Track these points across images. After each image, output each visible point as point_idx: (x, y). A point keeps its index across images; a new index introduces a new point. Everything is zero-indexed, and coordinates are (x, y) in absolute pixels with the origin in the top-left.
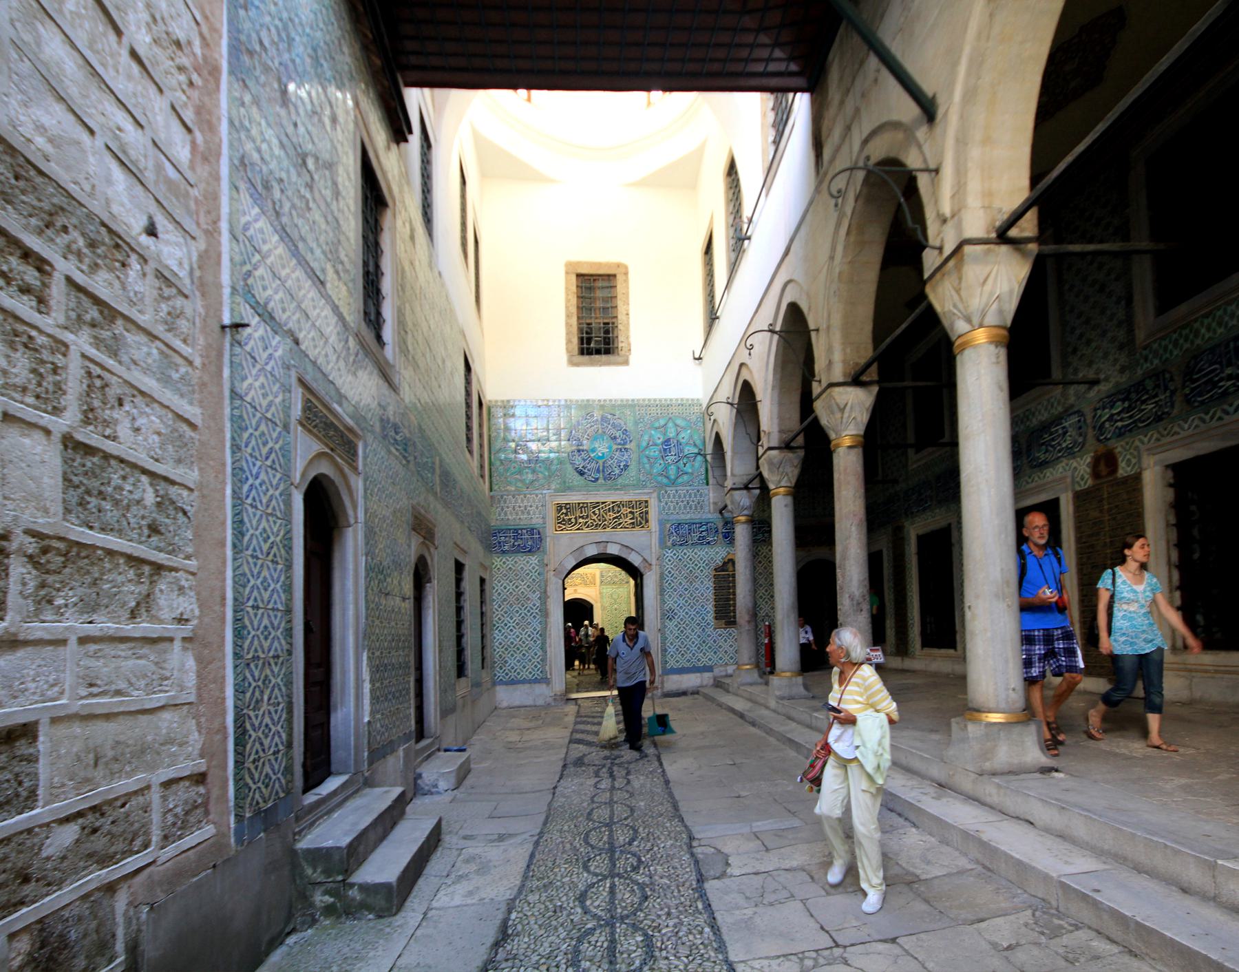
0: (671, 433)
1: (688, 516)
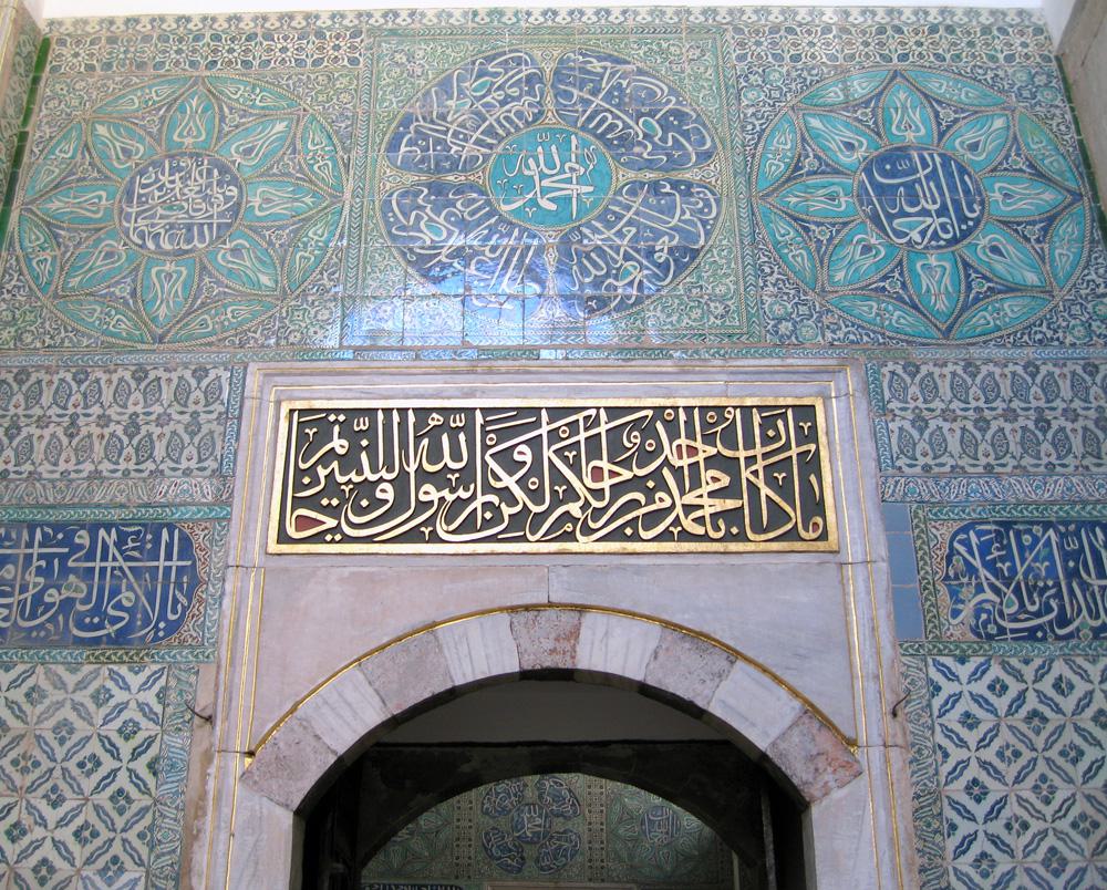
0: (911, 125)
1: (1056, 488)
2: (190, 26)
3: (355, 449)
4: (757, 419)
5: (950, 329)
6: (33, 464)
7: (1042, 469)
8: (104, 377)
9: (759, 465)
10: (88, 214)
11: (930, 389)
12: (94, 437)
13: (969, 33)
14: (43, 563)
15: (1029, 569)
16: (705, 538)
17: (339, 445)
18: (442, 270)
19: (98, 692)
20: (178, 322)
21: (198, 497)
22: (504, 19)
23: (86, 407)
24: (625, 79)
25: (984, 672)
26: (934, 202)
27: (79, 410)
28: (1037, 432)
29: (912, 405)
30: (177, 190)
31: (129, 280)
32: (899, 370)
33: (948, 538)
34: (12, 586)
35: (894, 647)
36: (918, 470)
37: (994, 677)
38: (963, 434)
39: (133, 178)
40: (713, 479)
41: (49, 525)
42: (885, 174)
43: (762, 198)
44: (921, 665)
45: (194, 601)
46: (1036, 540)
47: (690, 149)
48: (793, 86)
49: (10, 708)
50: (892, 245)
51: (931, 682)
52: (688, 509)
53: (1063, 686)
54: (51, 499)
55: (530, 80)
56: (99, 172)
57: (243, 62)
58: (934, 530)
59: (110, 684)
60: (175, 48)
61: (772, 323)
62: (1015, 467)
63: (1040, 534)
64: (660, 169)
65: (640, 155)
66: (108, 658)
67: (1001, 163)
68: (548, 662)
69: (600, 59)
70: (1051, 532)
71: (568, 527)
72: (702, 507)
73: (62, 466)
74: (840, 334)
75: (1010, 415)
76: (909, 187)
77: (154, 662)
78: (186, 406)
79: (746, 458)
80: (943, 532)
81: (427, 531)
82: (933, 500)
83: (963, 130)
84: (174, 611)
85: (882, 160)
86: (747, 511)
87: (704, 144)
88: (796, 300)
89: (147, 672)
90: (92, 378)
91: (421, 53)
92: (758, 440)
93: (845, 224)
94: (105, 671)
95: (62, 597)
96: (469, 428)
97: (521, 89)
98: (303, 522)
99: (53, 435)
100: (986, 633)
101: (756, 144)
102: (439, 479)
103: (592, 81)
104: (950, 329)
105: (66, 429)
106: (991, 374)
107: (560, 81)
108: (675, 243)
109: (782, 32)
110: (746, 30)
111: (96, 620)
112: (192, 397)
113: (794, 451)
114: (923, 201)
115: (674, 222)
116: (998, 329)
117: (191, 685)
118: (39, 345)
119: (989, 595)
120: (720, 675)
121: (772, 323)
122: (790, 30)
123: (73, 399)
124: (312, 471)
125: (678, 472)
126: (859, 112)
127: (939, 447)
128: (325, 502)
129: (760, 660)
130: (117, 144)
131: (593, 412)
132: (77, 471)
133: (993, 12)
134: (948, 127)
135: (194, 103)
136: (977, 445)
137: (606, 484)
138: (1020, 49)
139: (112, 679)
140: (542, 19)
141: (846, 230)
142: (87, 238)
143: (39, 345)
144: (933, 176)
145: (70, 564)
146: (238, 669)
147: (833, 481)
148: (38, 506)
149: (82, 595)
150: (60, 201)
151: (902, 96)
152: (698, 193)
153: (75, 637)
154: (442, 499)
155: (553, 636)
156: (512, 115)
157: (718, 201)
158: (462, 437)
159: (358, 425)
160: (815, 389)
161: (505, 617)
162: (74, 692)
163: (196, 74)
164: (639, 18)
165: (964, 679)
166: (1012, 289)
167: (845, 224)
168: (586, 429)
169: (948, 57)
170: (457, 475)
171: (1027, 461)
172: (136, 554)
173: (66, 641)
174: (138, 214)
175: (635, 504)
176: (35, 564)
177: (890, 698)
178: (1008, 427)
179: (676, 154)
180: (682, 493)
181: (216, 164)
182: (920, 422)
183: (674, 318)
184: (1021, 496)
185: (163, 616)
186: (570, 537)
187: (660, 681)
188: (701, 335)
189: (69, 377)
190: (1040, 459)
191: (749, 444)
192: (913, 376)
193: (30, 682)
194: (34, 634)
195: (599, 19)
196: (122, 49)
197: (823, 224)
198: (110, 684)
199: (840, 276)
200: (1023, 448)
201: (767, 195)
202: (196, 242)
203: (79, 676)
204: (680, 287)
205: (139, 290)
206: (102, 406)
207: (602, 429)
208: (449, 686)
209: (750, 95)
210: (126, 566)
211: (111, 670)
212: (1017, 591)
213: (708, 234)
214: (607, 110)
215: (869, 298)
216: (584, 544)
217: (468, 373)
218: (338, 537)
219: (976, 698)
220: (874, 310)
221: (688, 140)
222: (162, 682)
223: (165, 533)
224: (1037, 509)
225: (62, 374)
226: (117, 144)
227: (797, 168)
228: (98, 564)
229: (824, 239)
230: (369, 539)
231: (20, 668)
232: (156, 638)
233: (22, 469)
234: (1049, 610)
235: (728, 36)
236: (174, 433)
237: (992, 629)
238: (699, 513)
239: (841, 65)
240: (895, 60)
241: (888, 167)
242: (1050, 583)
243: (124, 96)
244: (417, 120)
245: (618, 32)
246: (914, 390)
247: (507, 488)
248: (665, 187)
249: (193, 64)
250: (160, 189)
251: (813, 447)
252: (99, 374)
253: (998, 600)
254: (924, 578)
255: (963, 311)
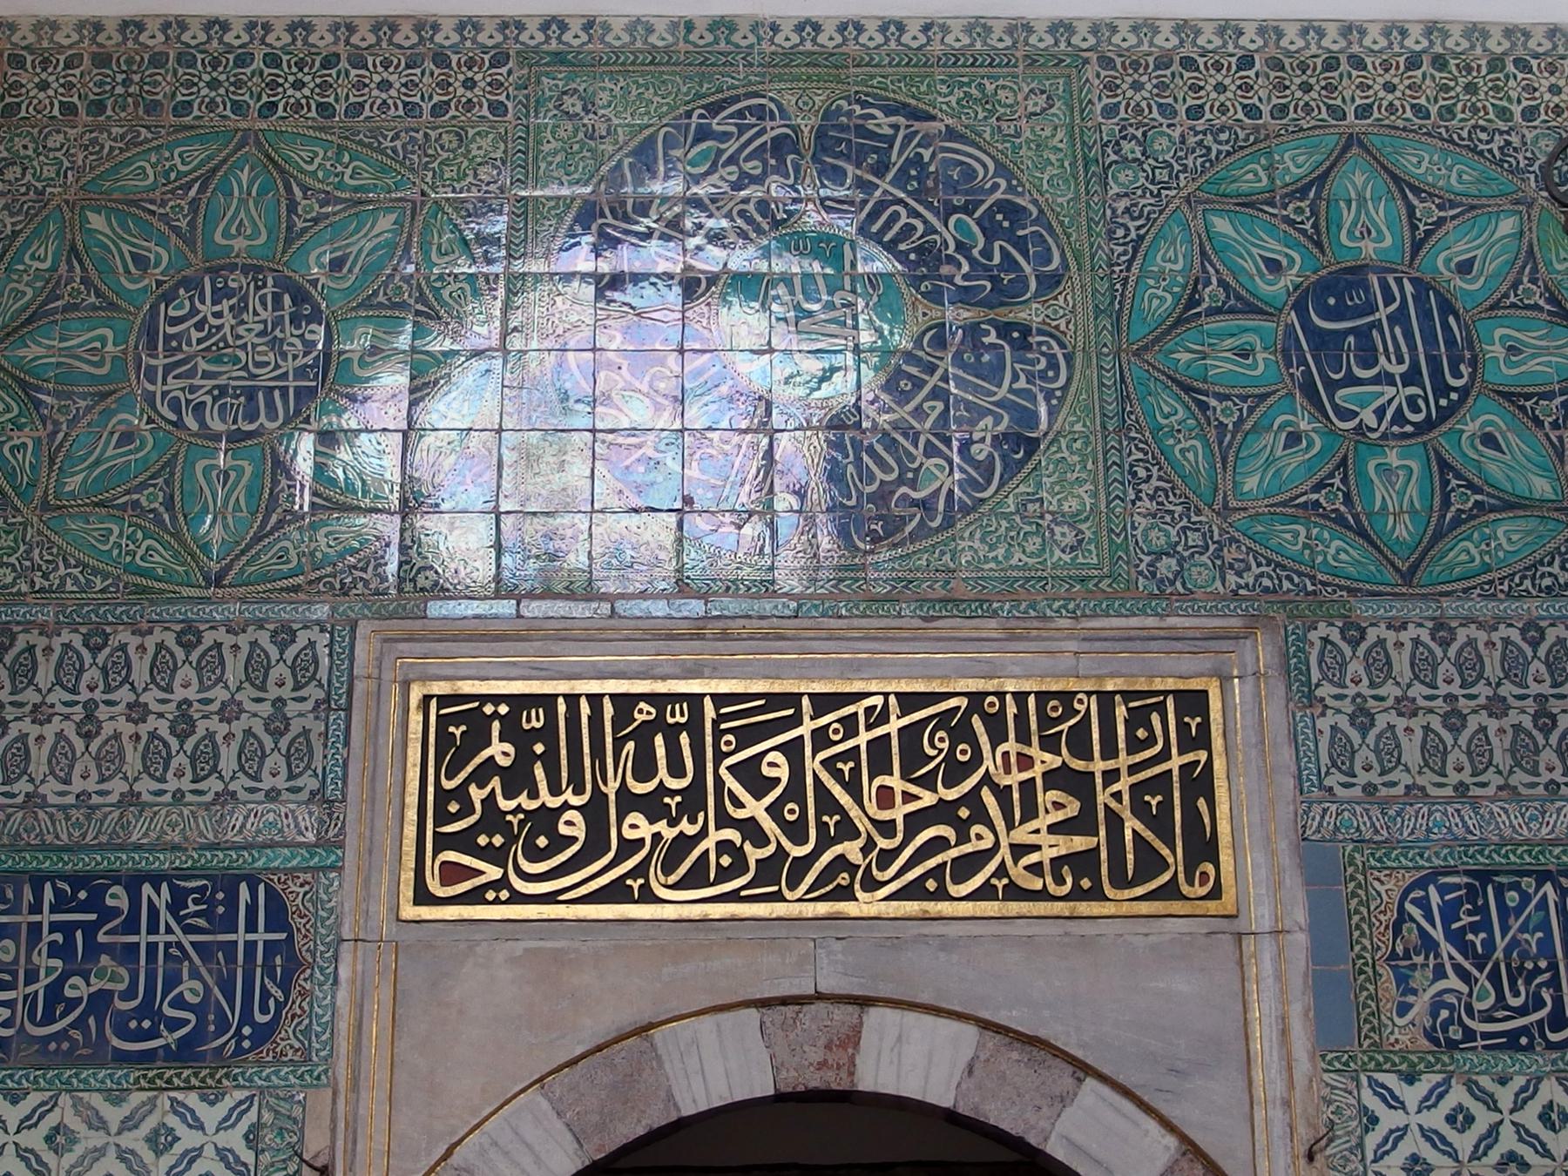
0: (1370, 229)
2: (228, 38)
3: (525, 757)
4: (1121, 712)
5: (1414, 568)
6: (31, 780)
7: (1540, 790)
8: (133, 642)
9: (1123, 785)
10: (86, 368)
11: (1379, 665)
12: (125, 739)
13: (1469, 69)
14: (59, 937)
15: (1514, 943)
16: (1043, 895)
17: (500, 751)
18: (648, 471)
19: (156, 1132)
20: (243, 553)
21: (290, 833)
22: (736, 38)
23: (108, 689)
24: (926, 148)
25: (1441, 1096)
26: (1400, 361)
27: (98, 695)
28: (1535, 732)
29: (1351, 690)
30: (227, 329)
31: (160, 480)
32: (1335, 636)
33: (1396, 896)
34: (14, 974)
35: (1312, 1058)
36: (1357, 792)
37: (1454, 1104)
38: (1426, 736)
39: (154, 308)
40: (1056, 805)
41: (64, 878)
42: (1328, 314)
43: (1137, 354)
44: (1352, 1086)
45: (293, 995)
46: (1525, 898)
47: (1028, 269)
48: (1190, 162)
49: (23, 1159)
50: (1332, 431)
51: (1364, 1110)
52: (1019, 850)
53: (1554, 1116)
54: (64, 837)
55: (781, 146)
56: (98, 295)
57: (319, 105)
58: (1376, 884)
59: (173, 1121)
60: (206, 78)
61: (1147, 559)
62: (1500, 788)
63: (1531, 891)
64: (979, 304)
65: (950, 279)
66: (169, 1081)
67: (1506, 295)
68: (815, 1081)
69: (888, 112)
70: (1548, 887)
71: (843, 879)
72: (1037, 848)
73: (77, 785)
74: (1249, 579)
75: (1496, 706)
76: (1362, 334)
77: (238, 1087)
78: (263, 688)
79: (1104, 773)
80: (1388, 888)
81: (636, 884)
82: (1376, 838)
83: (1451, 238)
84: (264, 1010)
85: (1324, 287)
86: (1104, 855)
87: (1049, 261)
88: (1184, 523)
89: (228, 1102)
90: (113, 642)
91: (605, 96)
92: (1122, 745)
93: (1263, 397)
94: (164, 1101)
95: (92, 989)
96: (694, 726)
97: (765, 163)
98: (452, 873)
99: (60, 735)
100: (1446, 1039)
101: (1130, 262)
102: (653, 807)
103: (876, 150)
104: (1414, 568)
105: (79, 725)
106: (1471, 642)
107: (825, 150)
108: (1001, 428)
109: (1176, 67)
110: (1119, 61)
111: (146, 1024)
112: (274, 674)
113: (1175, 762)
114: (1382, 359)
115: (1002, 392)
116: (1487, 569)
117: (295, 1121)
118: (25, 588)
119: (1454, 982)
120: (1064, 1100)
121: (1147, 559)
122: (1188, 63)
123: (86, 677)
124: (461, 793)
125: (1003, 794)
126: (1291, 206)
127: (1389, 755)
128: (482, 840)
129: (1121, 1079)
130: (125, 248)
131: (878, 701)
132: (101, 793)
133: (1509, 32)
134: (1428, 233)
135: (244, 177)
136: (1445, 752)
137: (898, 813)
138: (1547, 96)
139: (176, 1112)
140: (795, 39)
141: (1262, 408)
142: (89, 409)
143: (25, 588)
144: (1399, 318)
145: (102, 938)
146: (363, 1094)
147: (1226, 812)
148: (44, 847)
149: (122, 987)
150: (39, 344)
151: (1359, 179)
152: (1040, 344)
153: (115, 1048)
154: (657, 837)
155: (822, 1042)
156: (751, 207)
157: (1069, 358)
158: (684, 739)
159: (529, 720)
160: (1209, 666)
161: (753, 1013)
162: (119, 1133)
163: (243, 125)
164: (949, 39)
165: (1412, 1105)
166: (1512, 505)
167: (1263, 397)
168: (869, 728)
169: (1434, 110)
170: (678, 799)
171: (1519, 778)
172: (202, 922)
173: (99, 1055)
175: (939, 844)
176: (47, 937)
177: (1304, 1134)
178: (1493, 725)
179: (1006, 278)
180: (1010, 826)
181: (285, 285)
182: (1363, 717)
183: (1000, 552)
184: (1508, 832)
185: (247, 1017)
186: (846, 894)
187: (976, 1108)
188: (1041, 579)
189: (77, 641)
190: (1539, 775)
191: (1109, 751)
192: (1355, 643)
193: (52, 1120)
194: (53, 1046)
195: (887, 40)
196: (120, 77)
197: (1227, 397)
198: (173, 1121)
199: (1251, 484)
200: (1514, 757)
201: (1146, 348)
202: (262, 419)
203: (125, 1110)
204: (1010, 500)
205: (177, 498)
206: (133, 688)
207: (894, 725)
208: (673, 1117)
209: (1122, 177)
210: (187, 940)
211: (172, 1100)
212: (1494, 977)
213: (1052, 413)
214: (900, 202)
215: (1294, 519)
216: (866, 904)
217: (693, 637)
218: (504, 895)
219: (1428, 1135)
220: (1302, 539)
221: (1025, 254)
222: (252, 1115)
223: (243, 887)
224: (1529, 852)
225: (66, 637)
226: (125, 248)
227: (1193, 302)
228: (143, 939)
229: (1229, 422)
230: (550, 898)
231: (34, 1099)
232: (239, 1051)
233: (16, 788)
234: (1540, 1004)
235: (1090, 72)
236: (248, 732)
237: (1455, 1033)
238: (1033, 858)
239: (1264, 126)
240: (1351, 117)
241: (1332, 301)
242: (1543, 964)
243: (128, 162)
244: (603, 215)
245: (917, 62)
246: (1356, 667)
247: (752, 819)
248: (987, 333)
249: (238, 107)
250: (199, 326)
251: (1202, 756)
252: (124, 636)
253: (1465, 989)
254: (1360, 957)
255: (1438, 536)
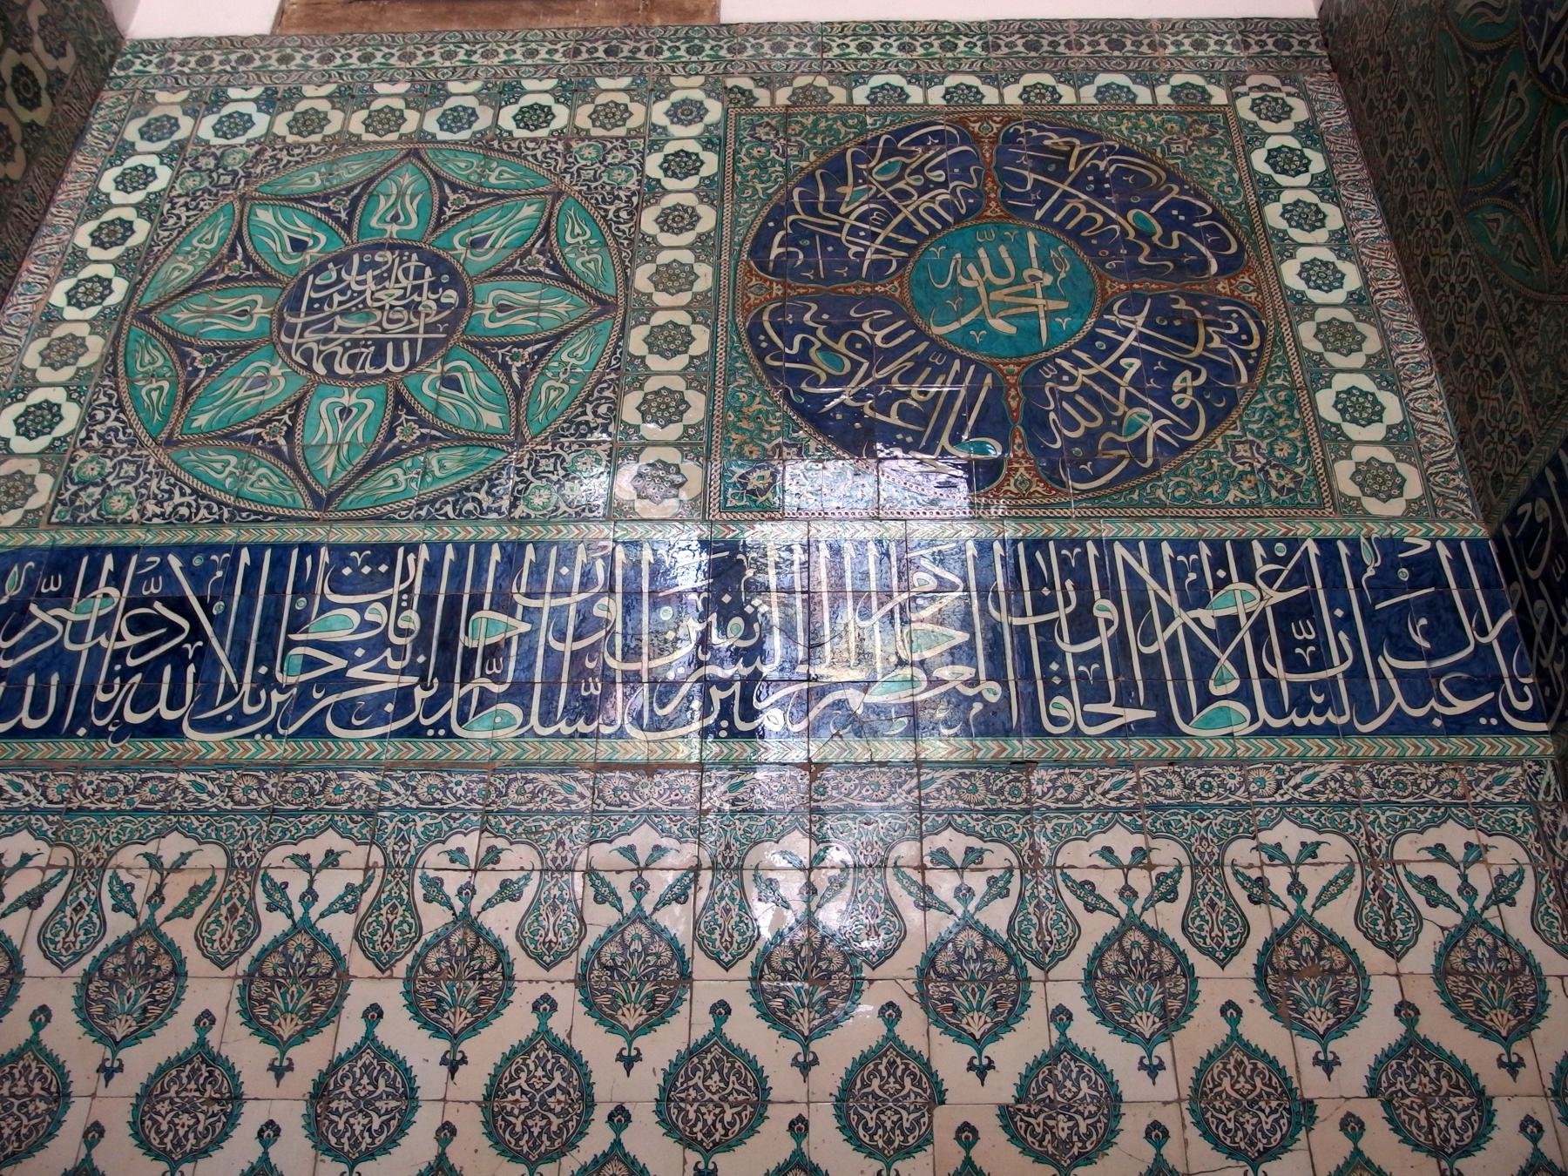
174: (306, 326)
250: (342, 292)
